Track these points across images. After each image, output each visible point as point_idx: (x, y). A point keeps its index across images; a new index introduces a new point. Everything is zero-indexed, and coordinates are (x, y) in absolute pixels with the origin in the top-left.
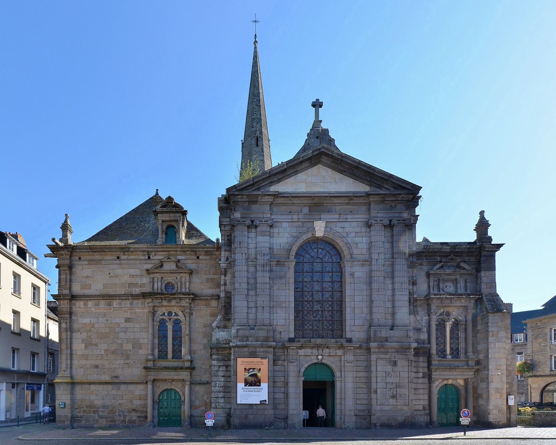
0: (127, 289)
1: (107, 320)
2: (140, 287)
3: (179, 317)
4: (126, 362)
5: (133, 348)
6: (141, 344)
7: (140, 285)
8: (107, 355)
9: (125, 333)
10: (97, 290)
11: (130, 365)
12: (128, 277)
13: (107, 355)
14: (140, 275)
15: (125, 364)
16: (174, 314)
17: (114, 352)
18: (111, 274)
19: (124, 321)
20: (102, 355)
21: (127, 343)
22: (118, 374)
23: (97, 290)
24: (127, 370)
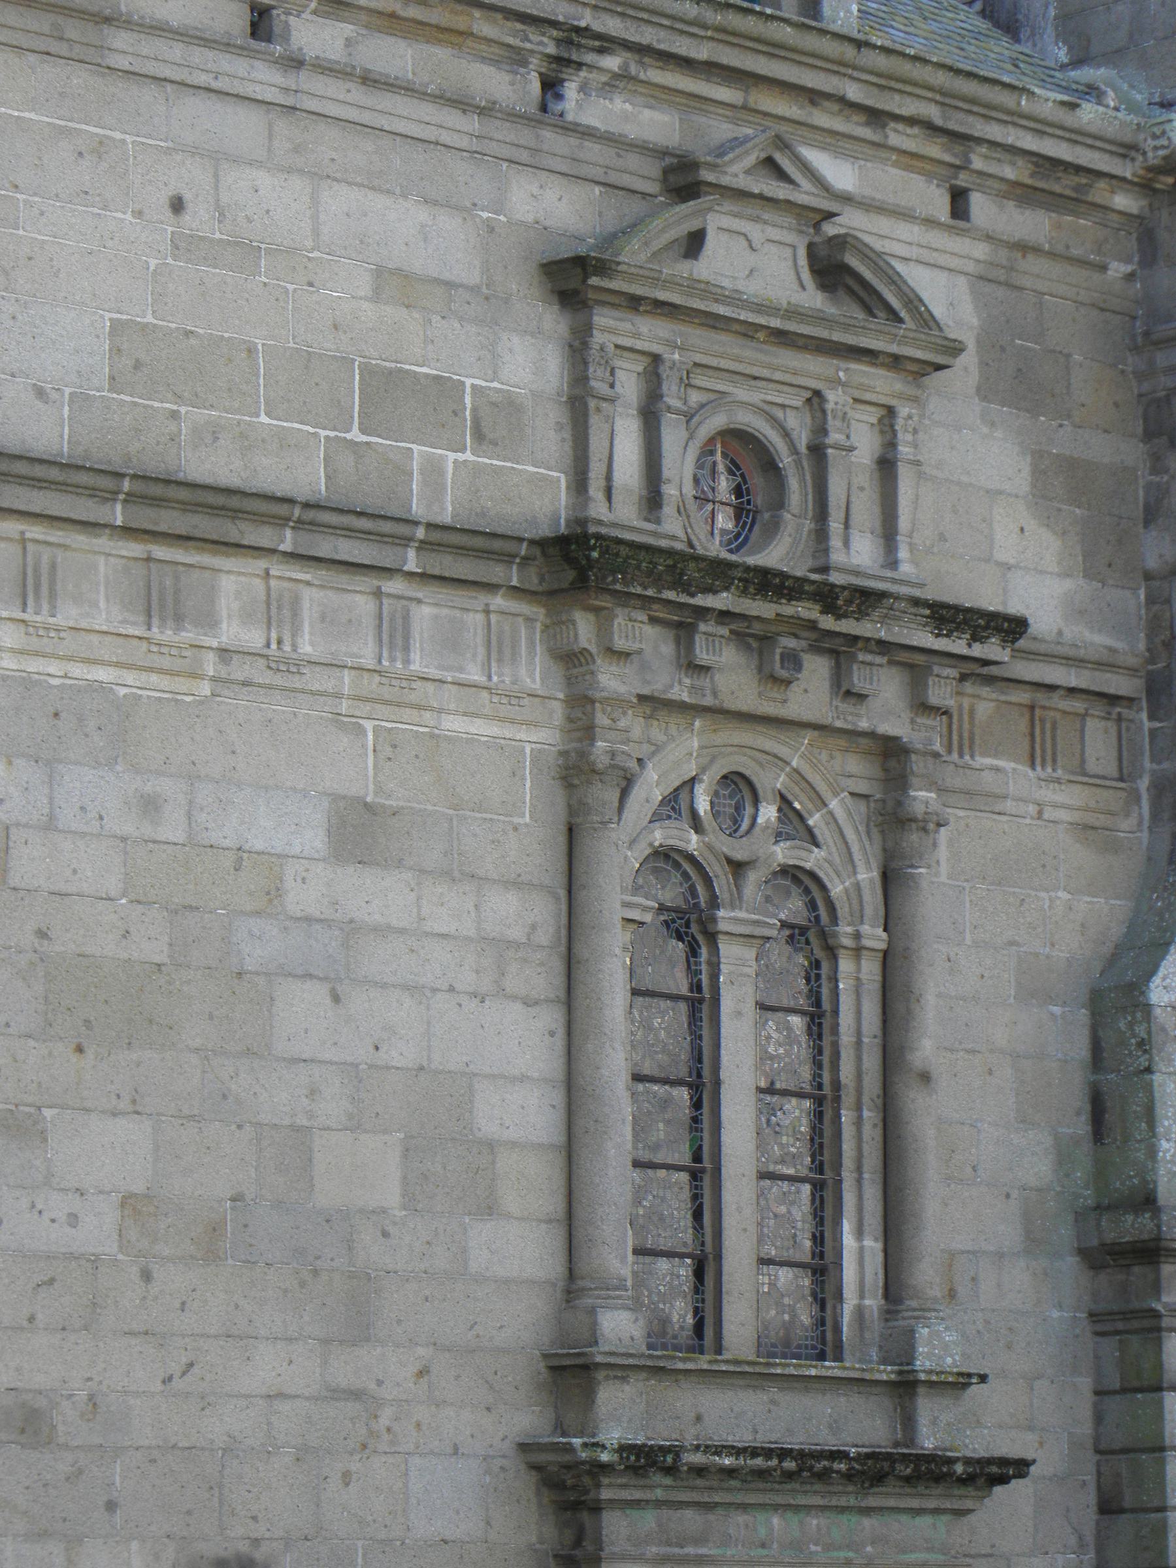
0: (355, 435)
1: (150, 806)
2: (479, 436)
3: (812, 859)
4: (343, 1372)
5: (409, 1201)
6: (491, 1146)
7: (474, 410)
8: (146, 1276)
9: (336, 998)
10: (40, 393)
11: (386, 1415)
12: (363, 284)
13: (146, 1276)
14: (474, 289)
15: (336, 1394)
16: (768, 813)
17: (216, 1229)
18: (198, 218)
19: (314, 840)
20: (95, 1261)
21: (354, 1125)
22: (260, 1530)
23: (40, 393)
24: (347, 1478)
